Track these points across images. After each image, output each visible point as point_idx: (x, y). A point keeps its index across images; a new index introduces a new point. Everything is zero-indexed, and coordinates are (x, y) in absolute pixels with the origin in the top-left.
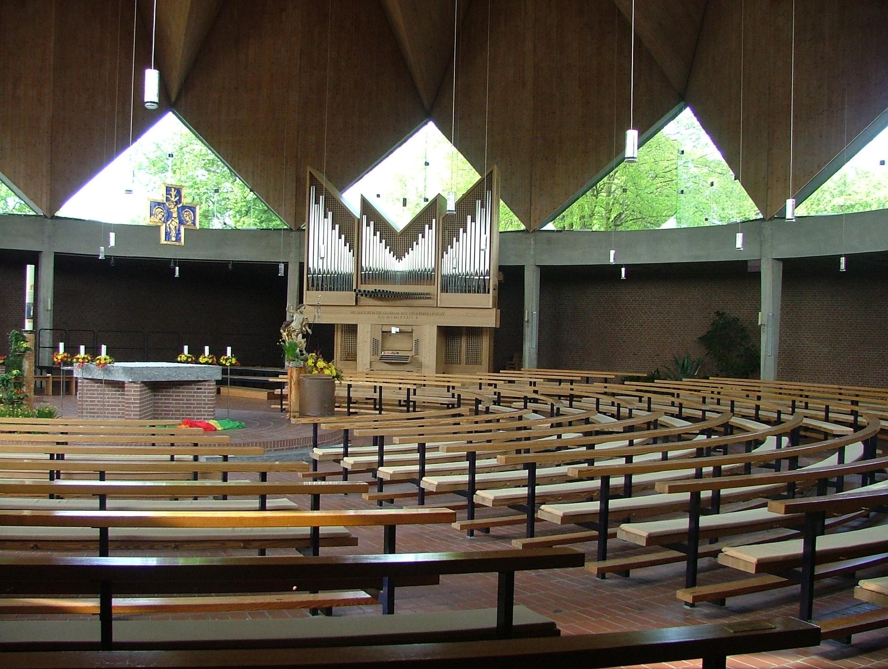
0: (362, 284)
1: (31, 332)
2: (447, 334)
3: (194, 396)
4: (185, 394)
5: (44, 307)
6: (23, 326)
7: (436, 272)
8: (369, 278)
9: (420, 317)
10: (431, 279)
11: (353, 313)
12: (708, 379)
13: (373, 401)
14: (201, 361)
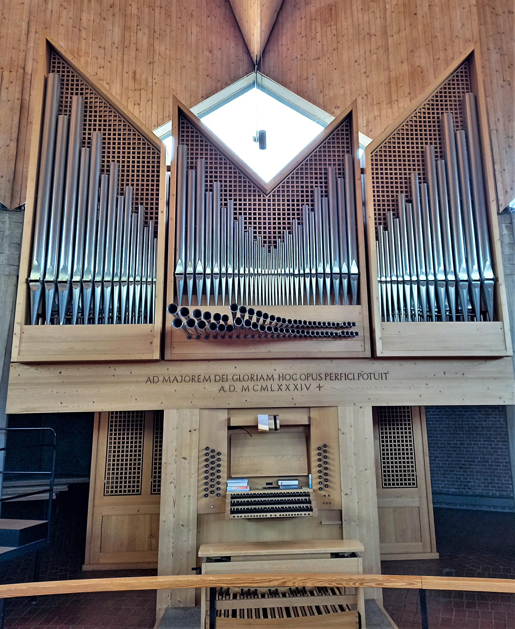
9: (328, 385)
11: (151, 380)
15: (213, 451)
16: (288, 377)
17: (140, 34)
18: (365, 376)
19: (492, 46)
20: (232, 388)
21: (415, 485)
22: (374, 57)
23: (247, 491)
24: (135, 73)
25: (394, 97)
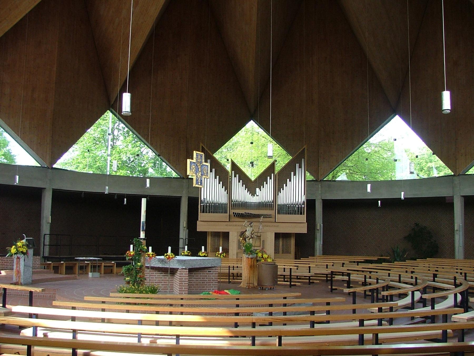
0: (232, 209)
1: (144, 239)
2: (277, 236)
3: (206, 276)
4: (201, 275)
5: (46, 221)
6: (139, 235)
7: (274, 203)
8: (234, 206)
10: (271, 207)
12: (416, 260)
13: (283, 277)
14: (200, 255)
21: (290, 253)
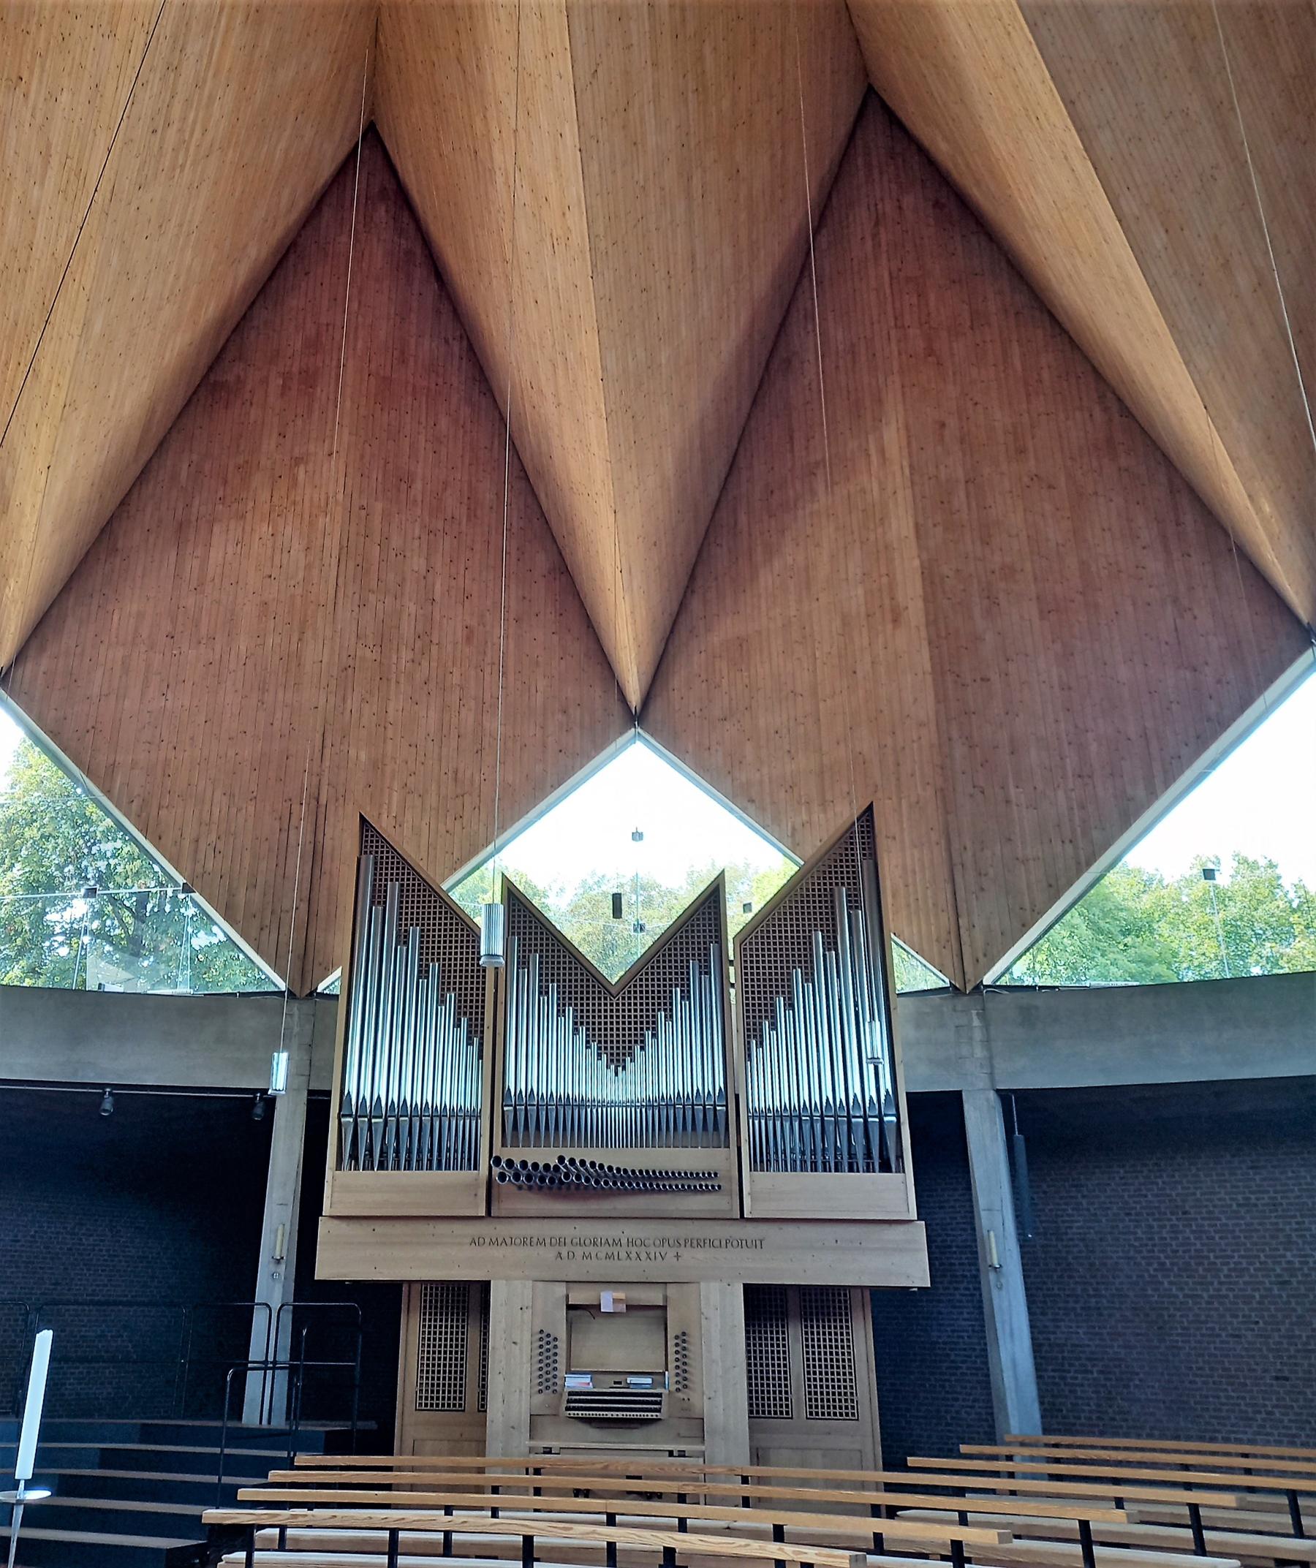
9: (687, 1253)
15: (548, 1335)
16: (638, 1242)
17: (464, 711)
18: (735, 1243)
19: (955, 735)
20: (571, 1254)
22: (801, 729)
23: (590, 1388)
24: (456, 772)
25: (829, 797)
